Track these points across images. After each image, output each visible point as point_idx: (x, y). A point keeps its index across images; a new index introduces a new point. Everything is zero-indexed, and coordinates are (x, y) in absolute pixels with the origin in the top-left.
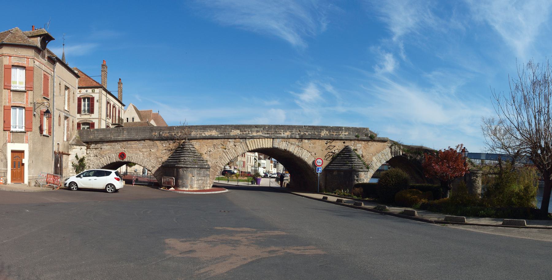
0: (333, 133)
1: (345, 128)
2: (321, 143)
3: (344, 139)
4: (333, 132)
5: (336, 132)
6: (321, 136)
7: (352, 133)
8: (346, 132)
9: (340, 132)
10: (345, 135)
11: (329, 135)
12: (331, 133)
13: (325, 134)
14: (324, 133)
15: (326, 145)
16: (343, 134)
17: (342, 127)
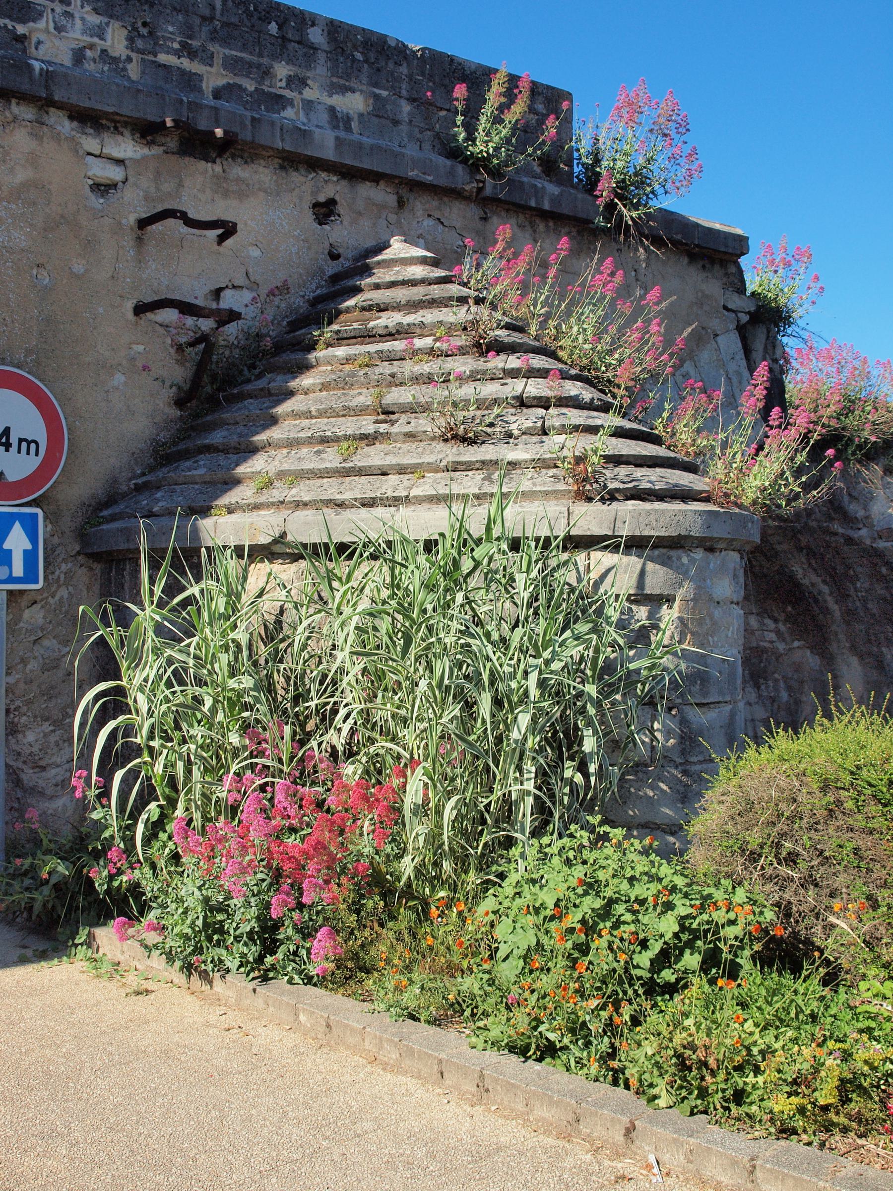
0: (186, 63)
1: (334, 28)
2: (33, 160)
3: (329, 153)
4: (192, 54)
5: (231, 65)
6: (37, 65)
7: (406, 108)
8: (345, 90)
9: (282, 70)
10: (338, 120)
11: (133, 71)
12: (163, 58)
13: (79, 56)
14: (76, 35)
15: (97, 202)
16: (309, 105)
17: (304, 19)
